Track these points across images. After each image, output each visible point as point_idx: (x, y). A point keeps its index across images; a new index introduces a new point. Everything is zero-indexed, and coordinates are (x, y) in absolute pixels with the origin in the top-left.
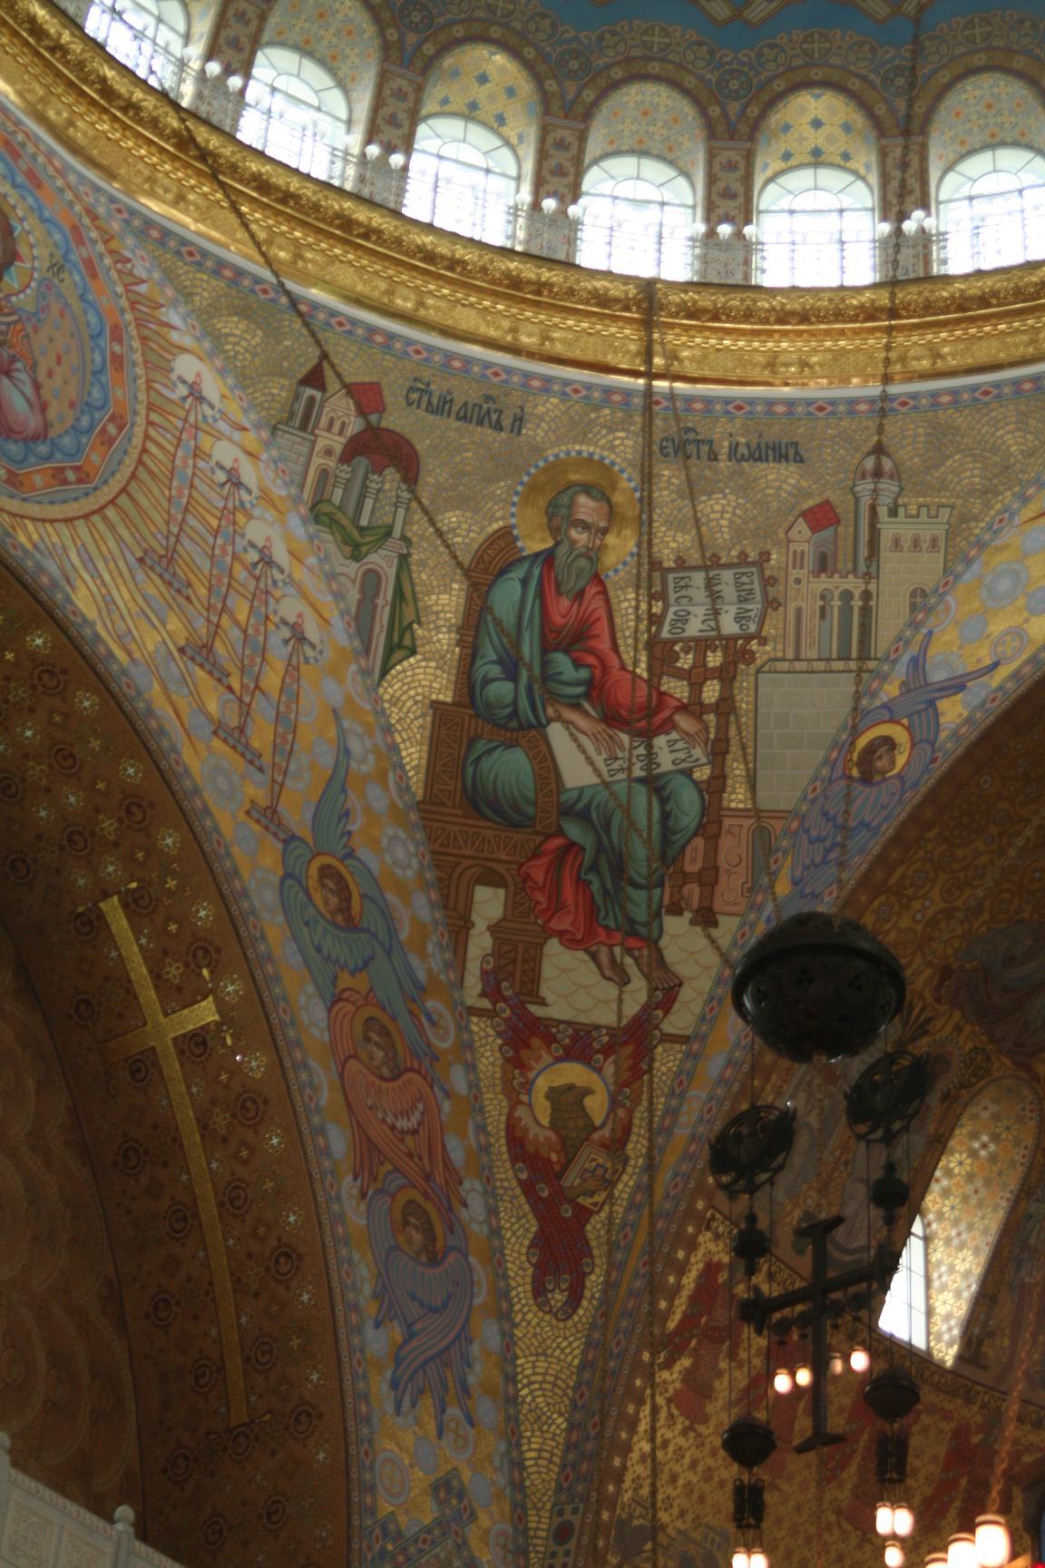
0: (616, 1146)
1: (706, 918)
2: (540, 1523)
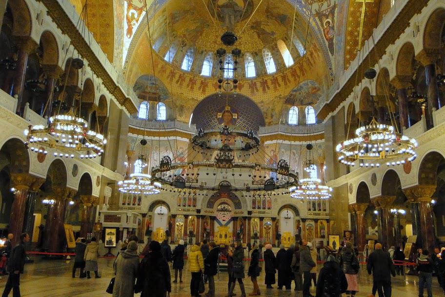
0: (137, 21)
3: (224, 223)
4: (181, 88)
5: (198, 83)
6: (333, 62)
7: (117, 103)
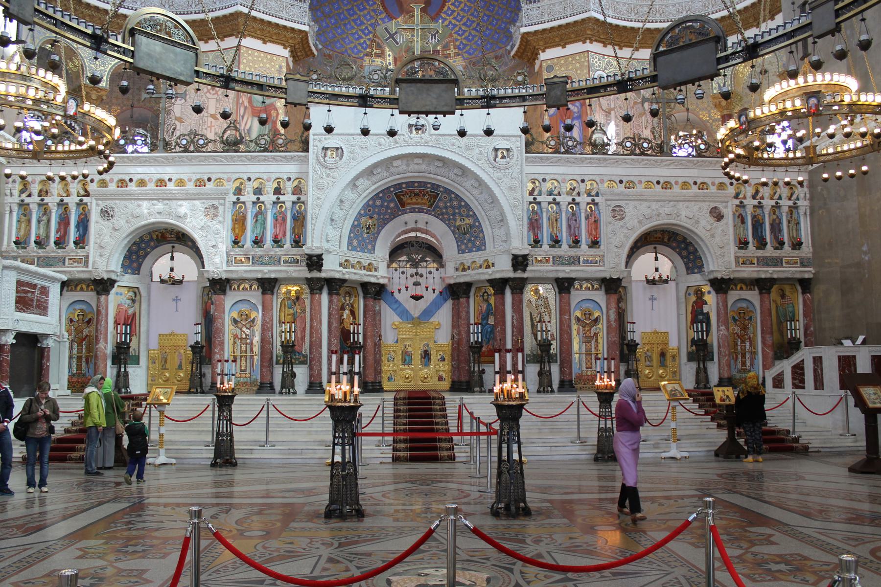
3: (416, 309)
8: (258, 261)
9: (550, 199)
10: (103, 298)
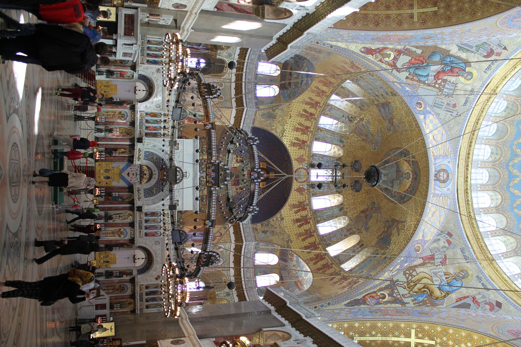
0: (381, 61)
1: (407, 78)
2: (334, 43)
3: (125, 174)
4: (298, 115)
5: (304, 137)
6: (338, 306)
7: (281, 33)
8: (141, 122)
9: (162, 219)
10: (130, 68)
